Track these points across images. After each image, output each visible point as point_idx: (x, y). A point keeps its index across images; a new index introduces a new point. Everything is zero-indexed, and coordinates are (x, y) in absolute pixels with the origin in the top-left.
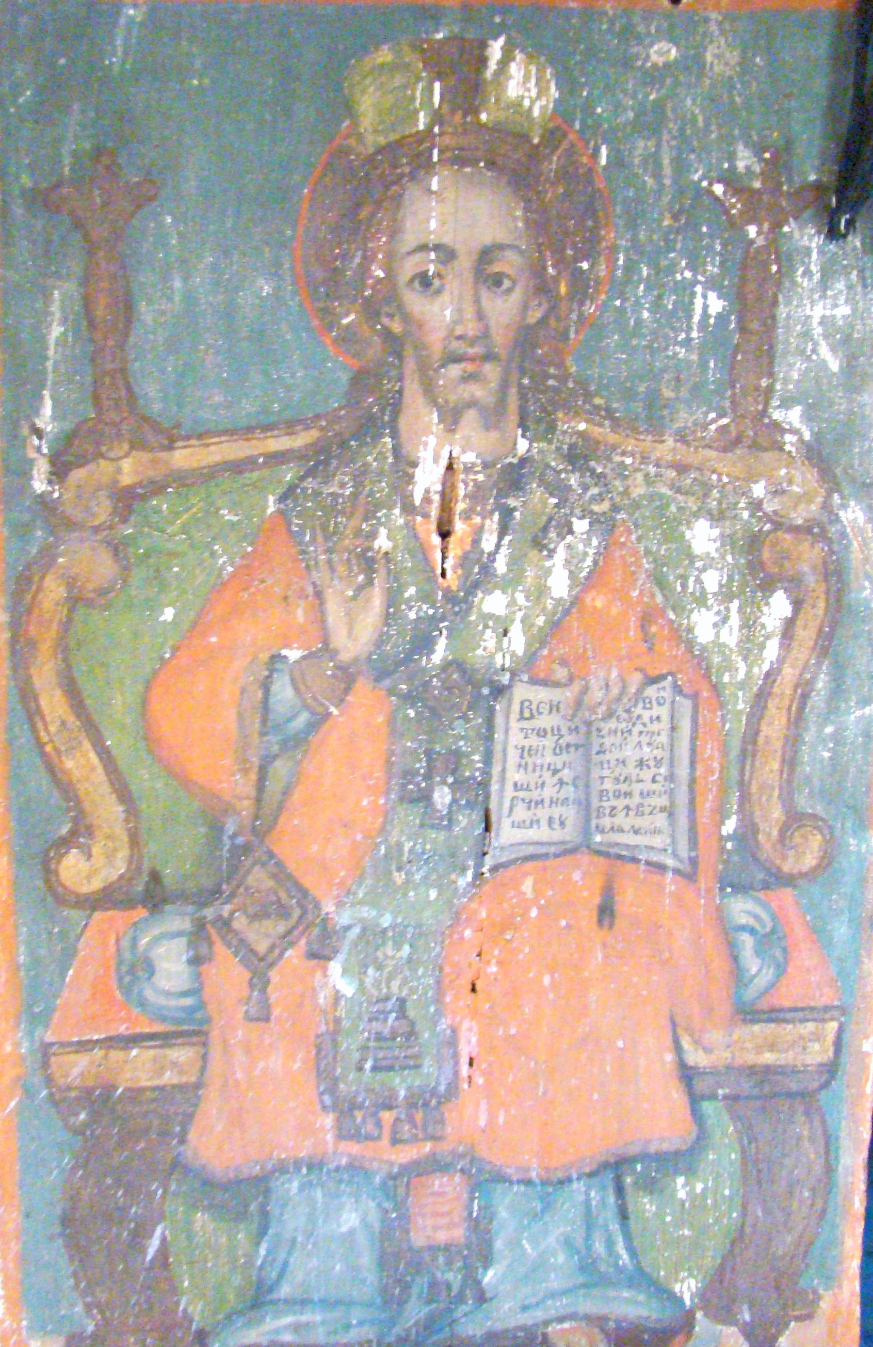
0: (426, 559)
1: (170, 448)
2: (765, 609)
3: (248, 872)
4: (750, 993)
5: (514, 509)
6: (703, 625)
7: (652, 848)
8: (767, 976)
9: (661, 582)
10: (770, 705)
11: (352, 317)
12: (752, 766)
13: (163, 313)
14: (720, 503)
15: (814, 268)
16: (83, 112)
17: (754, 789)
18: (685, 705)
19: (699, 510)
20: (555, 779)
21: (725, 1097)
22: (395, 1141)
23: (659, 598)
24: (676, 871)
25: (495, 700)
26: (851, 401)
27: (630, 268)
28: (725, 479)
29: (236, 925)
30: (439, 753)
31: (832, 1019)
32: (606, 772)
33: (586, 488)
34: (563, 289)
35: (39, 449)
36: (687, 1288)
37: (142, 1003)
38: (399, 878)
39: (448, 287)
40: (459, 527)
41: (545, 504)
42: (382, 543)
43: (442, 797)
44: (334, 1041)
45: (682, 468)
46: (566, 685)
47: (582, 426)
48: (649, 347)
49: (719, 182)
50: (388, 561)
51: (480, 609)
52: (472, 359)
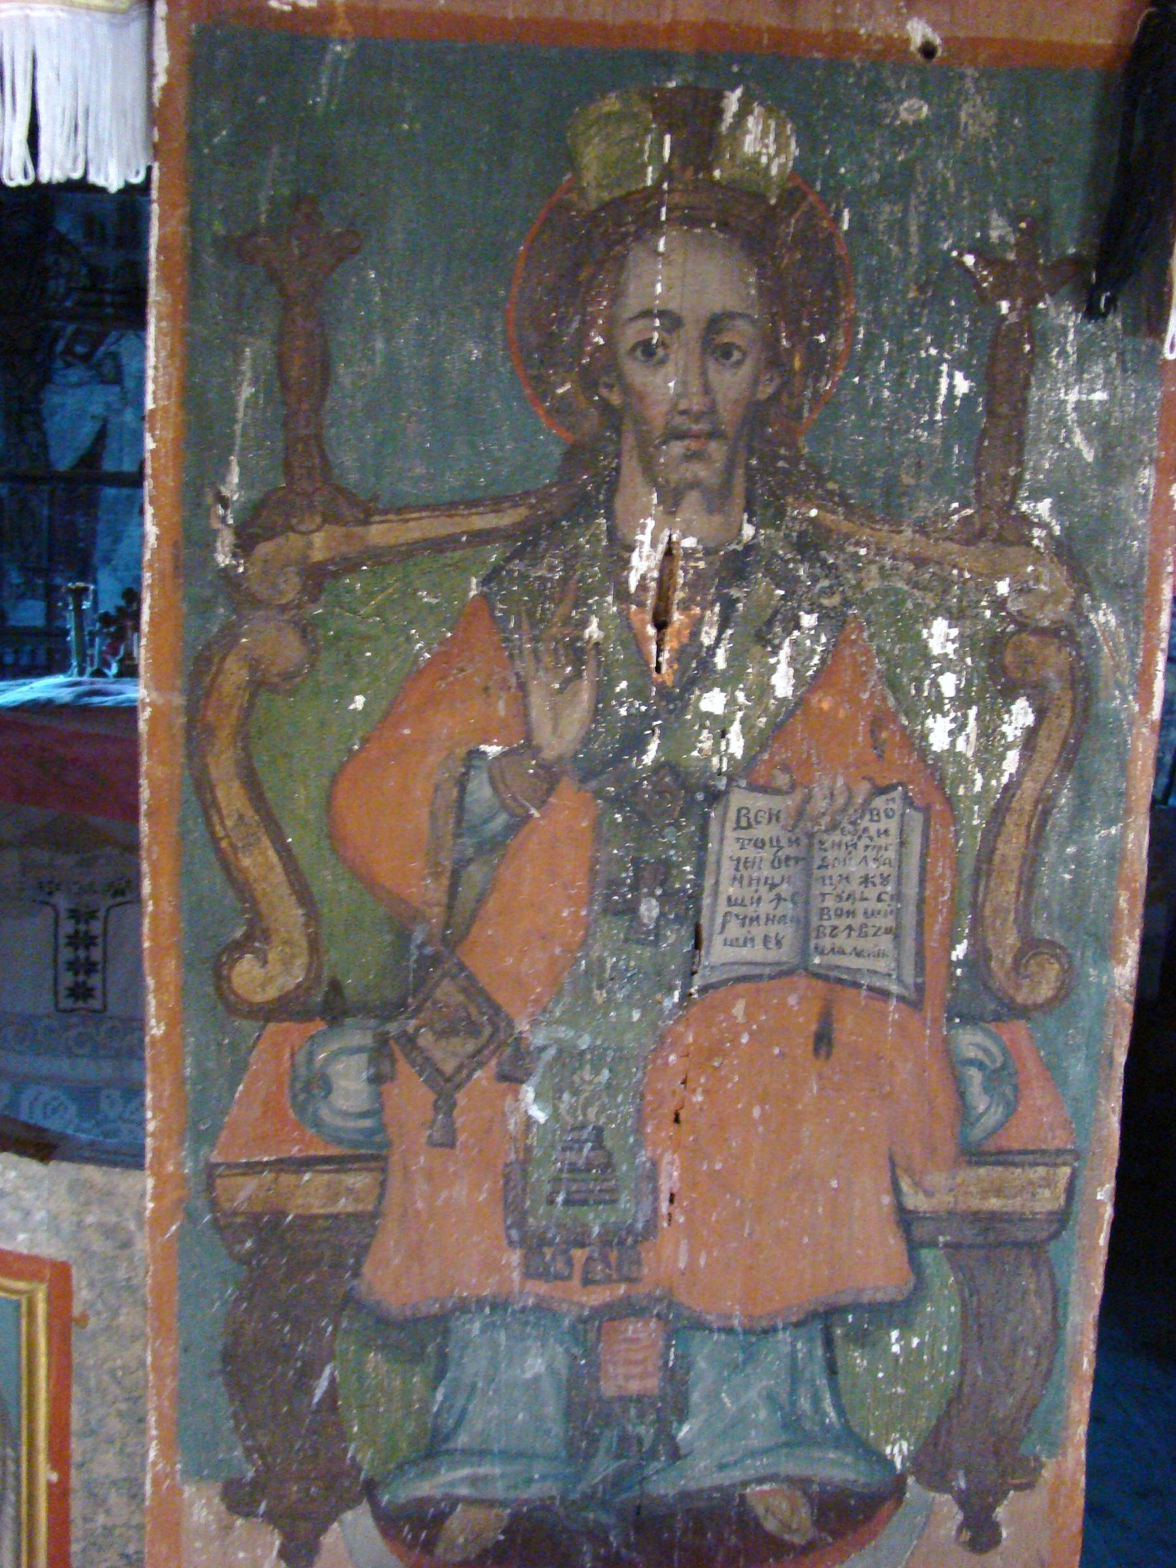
0: (641, 653)
1: (366, 522)
2: (1006, 717)
3: (437, 985)
4: (977, 1133)
5: (738, 600)
6: (937, 732)
7: (875, 972)
8: (996, 1115)
9: (894, 685)
10: (1008, 821)
11: (568, 386)
12: (987, 886)
13: (363, 376)
14: (960, 601)
15: (1069, 349)
16: (282, 155)
17: (987, 911)
18: (916, 819)
19: (938, 607)
20: (772, 895)
21: (946, 1245)
22: (587, 1281)
23: (891, 702)
24: (901, 999)
25: (710, 806)
26: (1105, 494)
27: (871, 342)
28: (967, 575)
29: (421, 1042)
30: (647, 862)
31: (1065, 1164)
32: (828, 889)
33: (815, 580)
34: (797, 364)
35: (223, 520)
36: (898, 1451)
37: (317, 1123)
38: (600, 996)
39: (672, 357)
40: (677, 616)
41: (771, 596)
42: (593, 631)
43: (649, 910)
44: (524, 1170)
45: (920, 562)
46: (787, 793)
47: (814, 513)
48: (889, 429)
49: (970, 252)
50: (599, 652)
51: (697, 707)
52: (696, 436)
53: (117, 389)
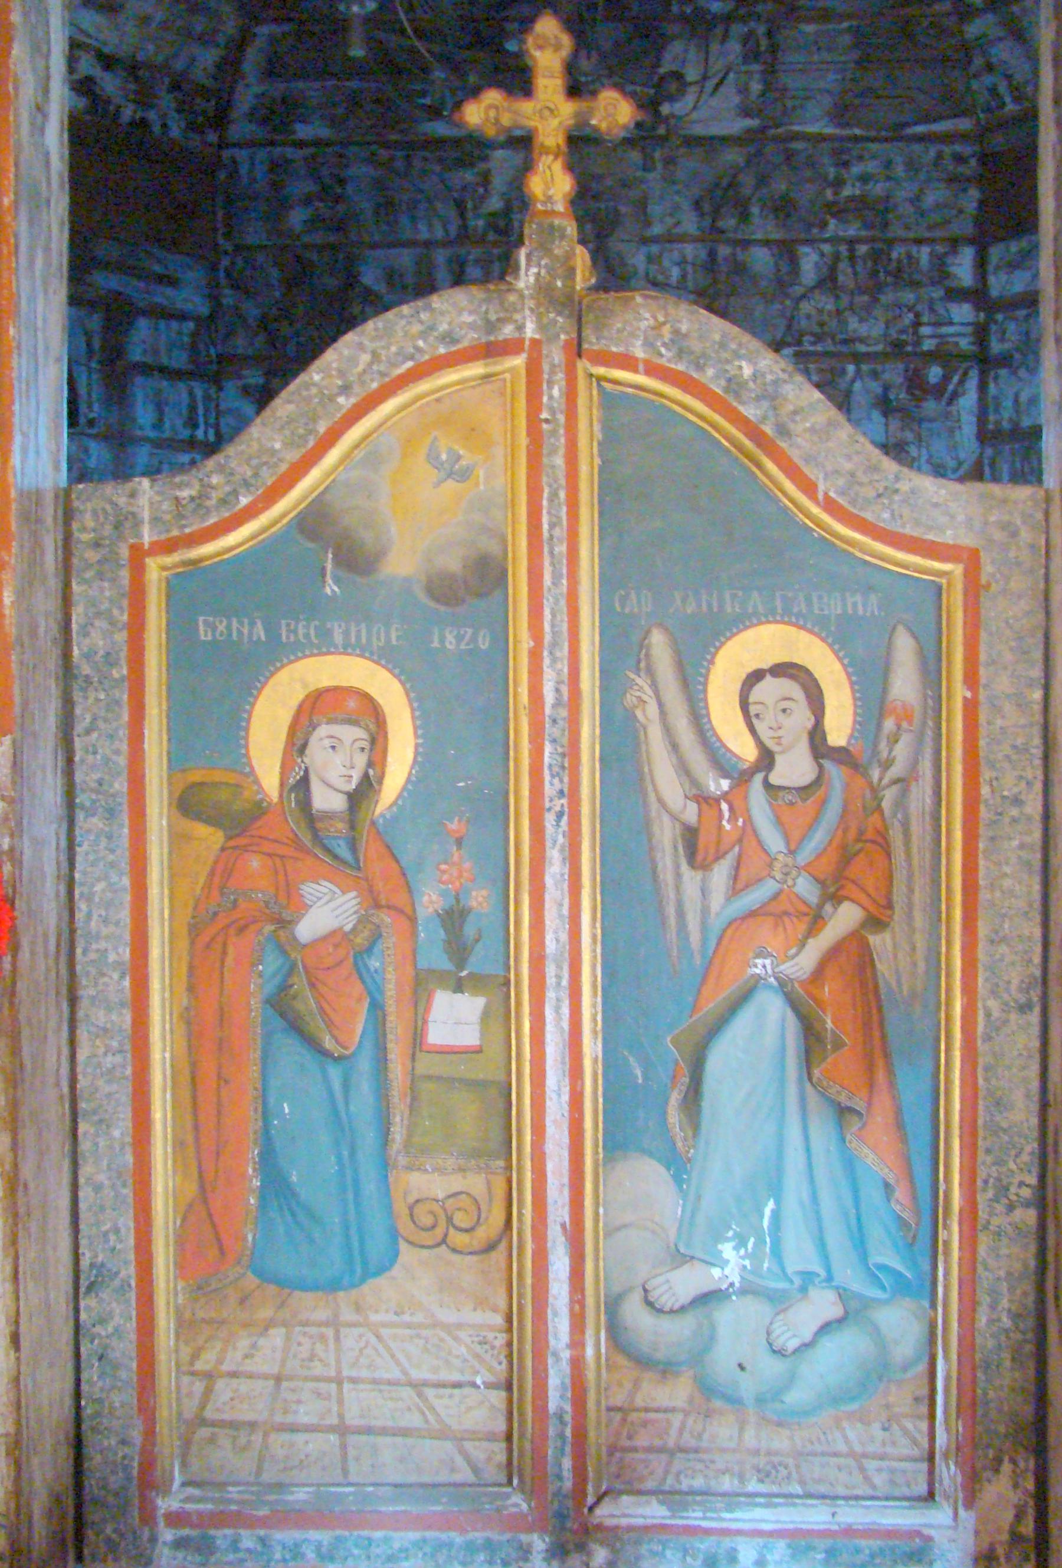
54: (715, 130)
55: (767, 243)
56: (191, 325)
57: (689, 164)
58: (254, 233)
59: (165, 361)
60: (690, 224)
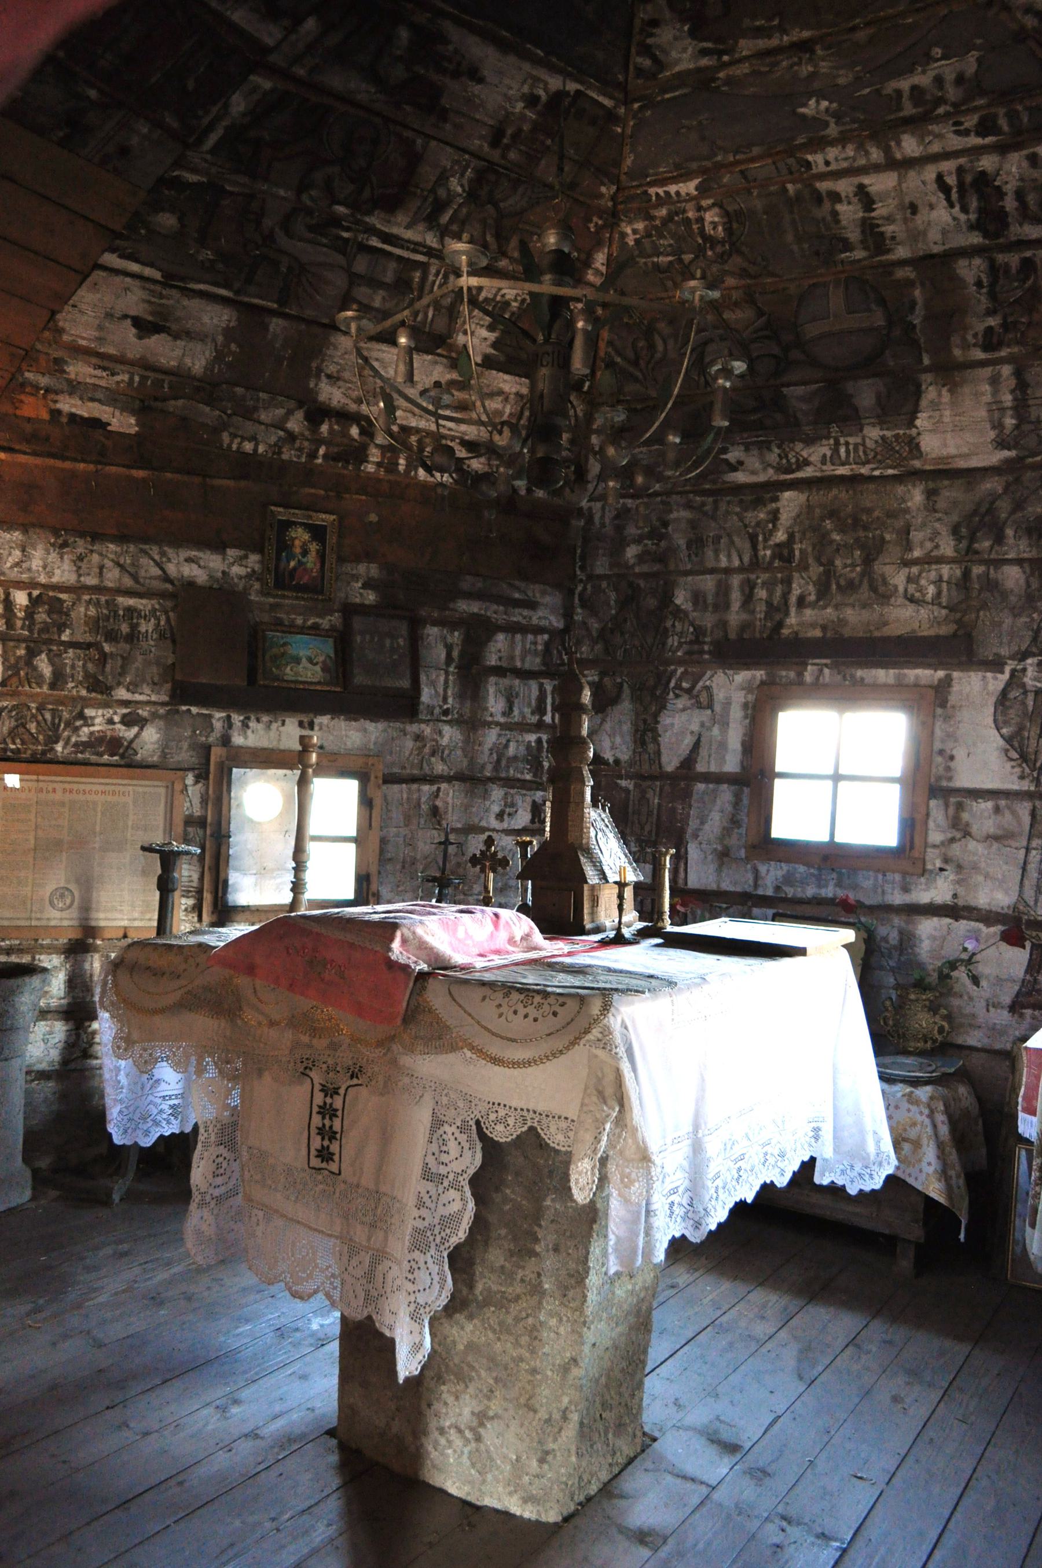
53: (709, 712)
54: (975, 463)
55: (1019, 562)
56: (546, 637)
57: (950, 493)
58: (601, 566)
59: (519, 664)
60: (947, 547)
